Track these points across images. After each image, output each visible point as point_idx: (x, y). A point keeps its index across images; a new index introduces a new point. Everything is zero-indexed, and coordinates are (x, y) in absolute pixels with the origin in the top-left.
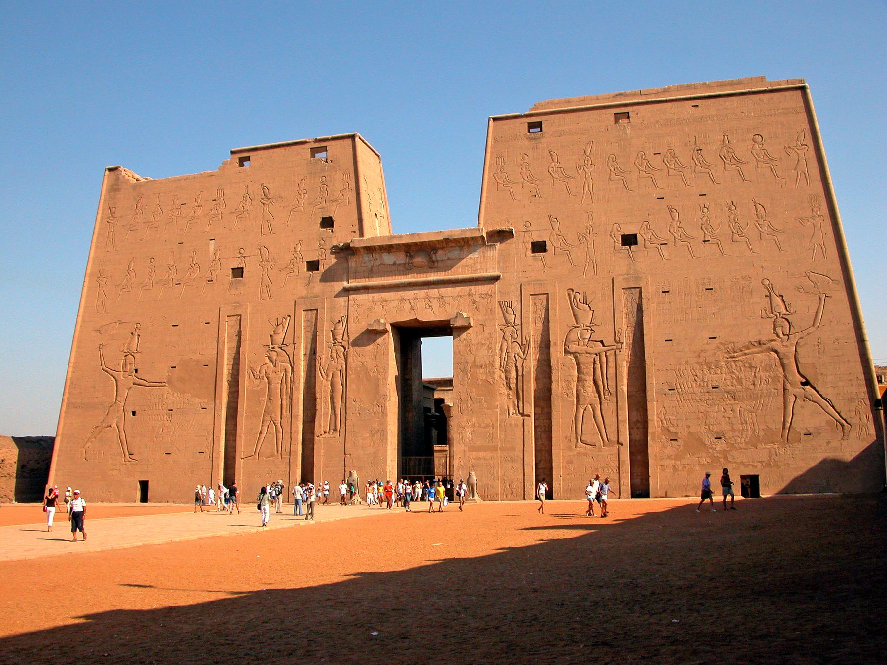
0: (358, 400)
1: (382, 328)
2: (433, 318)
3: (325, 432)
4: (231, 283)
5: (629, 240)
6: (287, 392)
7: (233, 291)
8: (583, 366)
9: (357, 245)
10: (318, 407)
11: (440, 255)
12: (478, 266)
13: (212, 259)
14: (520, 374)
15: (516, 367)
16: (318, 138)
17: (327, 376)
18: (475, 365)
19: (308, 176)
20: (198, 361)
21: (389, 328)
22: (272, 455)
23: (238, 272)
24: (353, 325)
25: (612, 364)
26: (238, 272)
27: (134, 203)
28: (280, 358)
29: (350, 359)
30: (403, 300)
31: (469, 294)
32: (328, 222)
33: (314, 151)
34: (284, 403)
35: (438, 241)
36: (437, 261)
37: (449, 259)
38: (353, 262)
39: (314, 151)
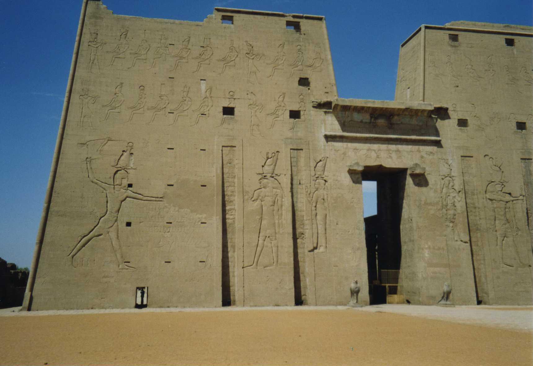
1: (361, 169)
5: (521, 126)
7: (225, 125)
13: (204, 97)
16: (294, 14)
18: (426, 204)
19: (286, 43)
23: (228, 111)
26: (228, 111)
27: (119, 34)
31: (418, 151)
32: (304, 82)
33: (289, 24)
35: (399, 109)
36: (394, 124)
37: (402, 123)
39: (289, 24)
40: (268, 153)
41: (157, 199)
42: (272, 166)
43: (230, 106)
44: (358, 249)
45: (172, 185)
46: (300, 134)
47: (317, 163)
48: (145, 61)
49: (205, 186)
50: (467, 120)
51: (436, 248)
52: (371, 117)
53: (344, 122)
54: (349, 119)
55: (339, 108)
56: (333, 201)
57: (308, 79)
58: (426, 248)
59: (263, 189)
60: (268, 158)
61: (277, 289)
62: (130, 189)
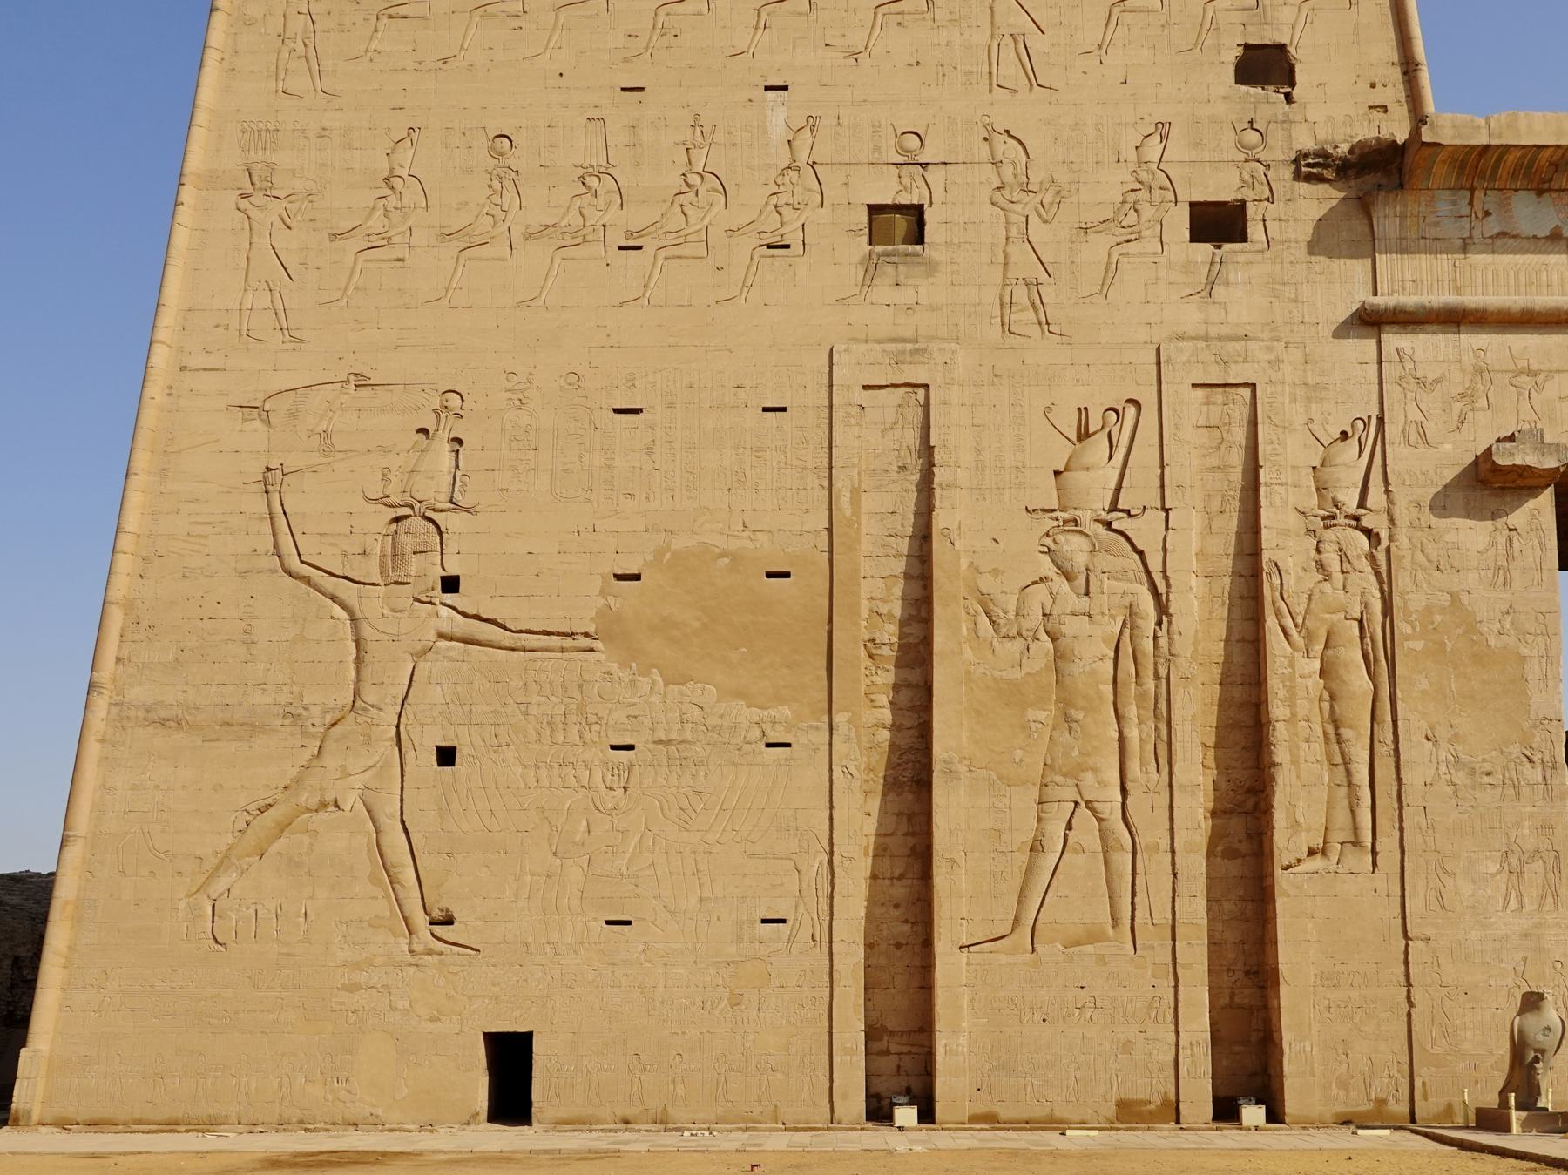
0: (1443, 733)
4: (871, 267)
6: (1141, 698)
7: (883, 292)
10: (1281, 754)
17: (1309, 638)
20: (736, 558)
22: (1094, 937)
24: (1405, 451)
28: (1103, 562)
29: (1402, 581)
32: (1265, 66)
34: (1133, 734)
38: (1387, 218)
40: (1083, 412)
41: (568, 642)
43: (904, 199)
45: (637, 577)
48: (515, 23)
49: (787, 575)
56: (1409, 630)
57: (1282, 48)
59: (1061, 585)
60: (1084, 434)
61: (1127, 1047)
62: (449, 598)
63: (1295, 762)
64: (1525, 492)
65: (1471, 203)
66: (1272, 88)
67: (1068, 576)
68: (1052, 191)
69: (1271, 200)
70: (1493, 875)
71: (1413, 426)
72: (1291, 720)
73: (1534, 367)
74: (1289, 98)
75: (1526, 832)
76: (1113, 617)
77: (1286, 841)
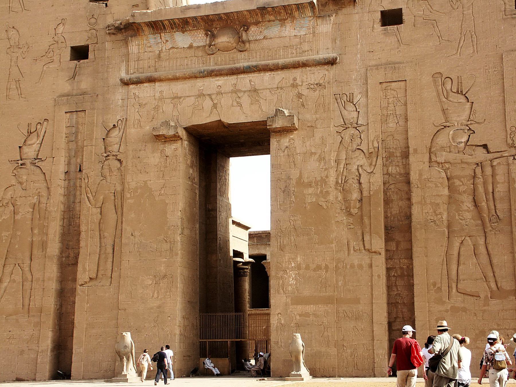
1: (171, 132)
2: (242, 119)
3: (91, 279)
8: (457, 182)
9: (138, 20)
10: (82, 244)
11: (254, 32)
12: (306, 47)
14: (365, 193)
15: (360, 183)
18: (300, 182)
21: (182, 133)
25: (500, 178)
29: (129, 178)
30: (201, 95)
35: (249, 11)
36: (249, 41)
42: (36, 147)
44: (165, 276)
46: (85, 83)
47: (109, 131)
50: (401, 9)
51: (313, 266)
52: (207, 35)
53: (160, 52)
54: (169, 45)
55: (146, 29)
58: (292, 269)
60: (30, 133)
63: (87, 246)
64: (172, 142)
65: (161, 38)
66: (102, 2)
67: (21, 183)
68: (26, 47)
69: (97, 43)
70: (150, 285)
71: (137, 121)
72: (87, 231)
73: (179, 96)
74: (106, 4)
75: (162, 268)
76: (33, 197)
77: (82, 276)
